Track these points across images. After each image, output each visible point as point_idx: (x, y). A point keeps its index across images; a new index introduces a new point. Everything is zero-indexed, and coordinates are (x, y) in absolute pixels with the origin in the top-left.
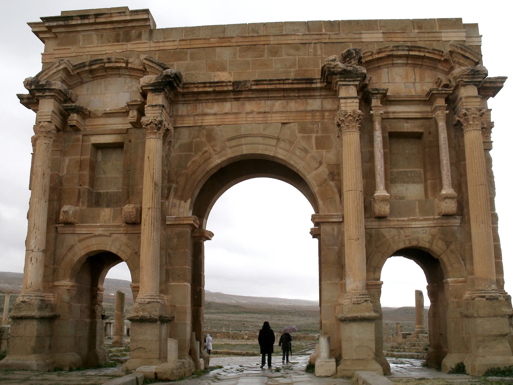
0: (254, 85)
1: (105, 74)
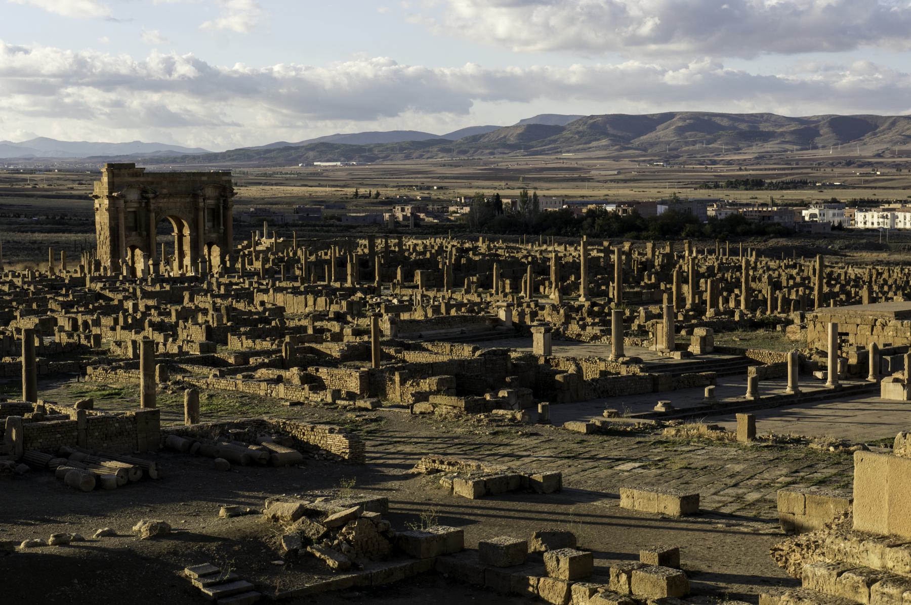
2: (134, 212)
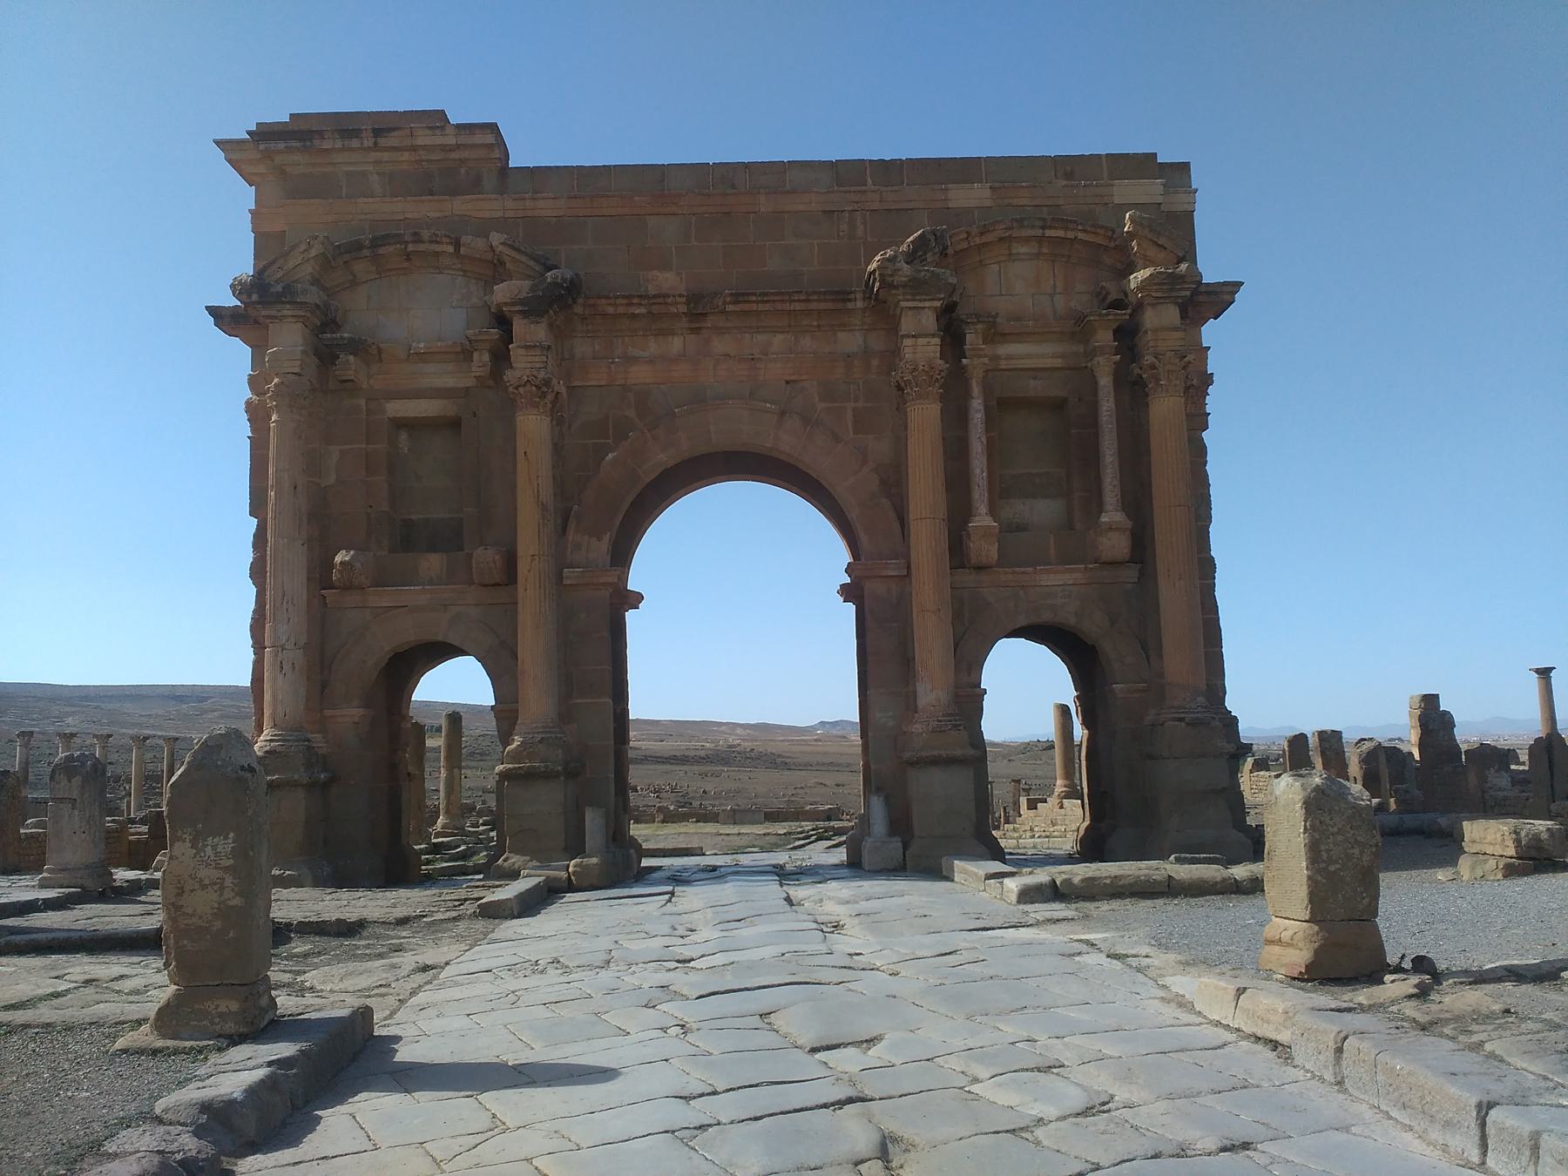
0: (729, 303)
1: (406, 264)
2: (453, 424)
